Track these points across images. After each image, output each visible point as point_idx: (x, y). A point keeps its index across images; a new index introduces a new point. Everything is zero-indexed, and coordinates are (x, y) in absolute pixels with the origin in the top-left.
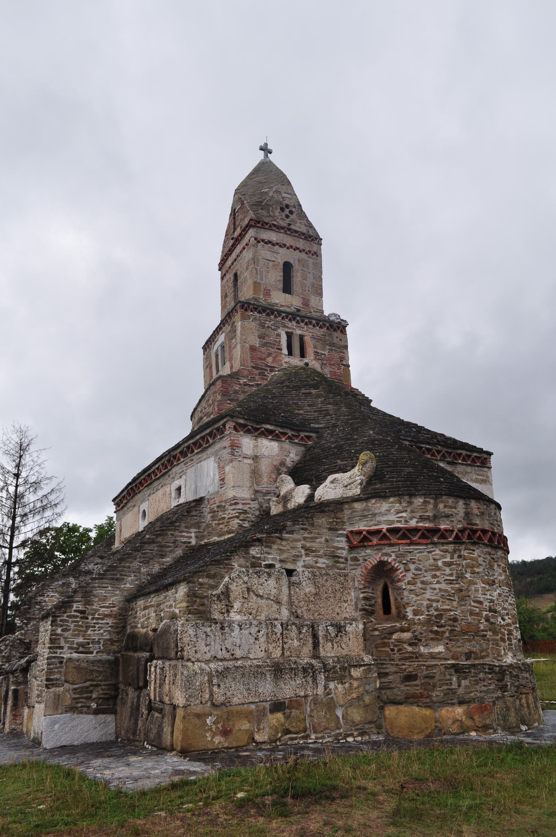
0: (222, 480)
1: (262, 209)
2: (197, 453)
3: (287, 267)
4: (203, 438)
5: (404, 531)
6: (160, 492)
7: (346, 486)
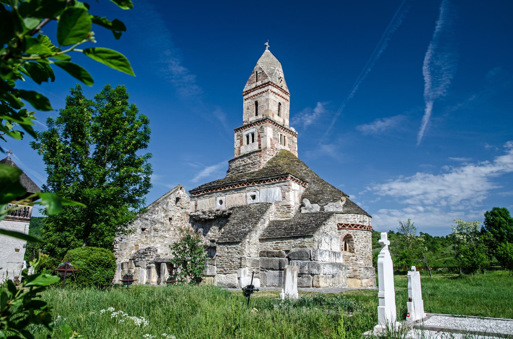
3: (280, 104)
6: (236, 195)
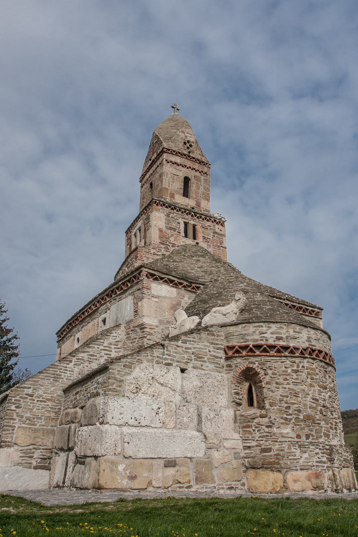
0: (136, 311)
1: (172, 142)
2: (119, 295)
3: (187, 180)
4: (123, 284)
5: (265, 346)
6: (90, 325)
7: (225, 315)
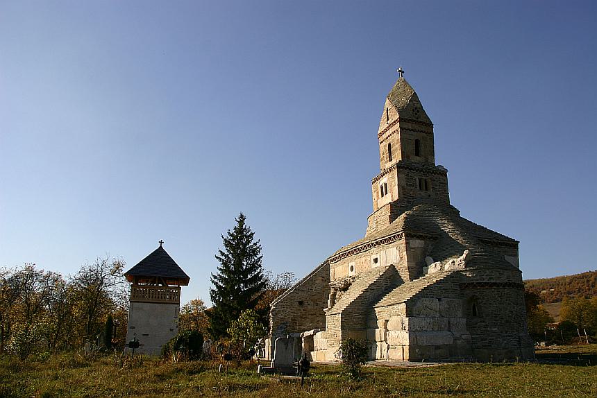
3: (417, 141)
6: (363, 259)
